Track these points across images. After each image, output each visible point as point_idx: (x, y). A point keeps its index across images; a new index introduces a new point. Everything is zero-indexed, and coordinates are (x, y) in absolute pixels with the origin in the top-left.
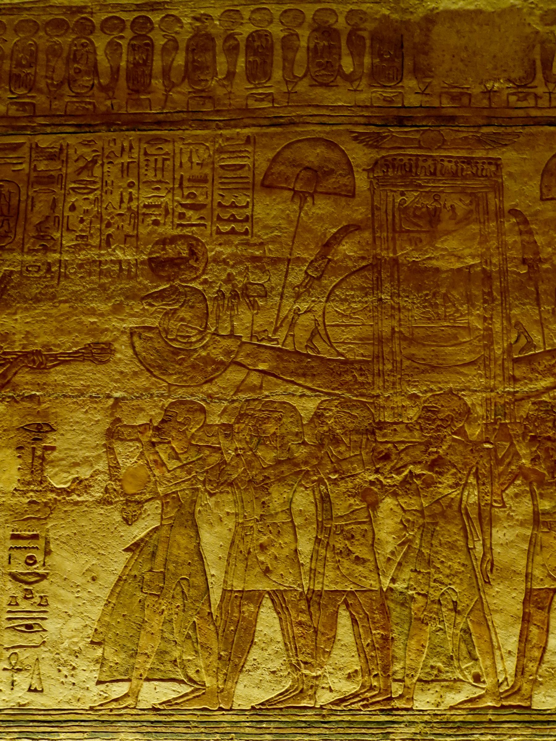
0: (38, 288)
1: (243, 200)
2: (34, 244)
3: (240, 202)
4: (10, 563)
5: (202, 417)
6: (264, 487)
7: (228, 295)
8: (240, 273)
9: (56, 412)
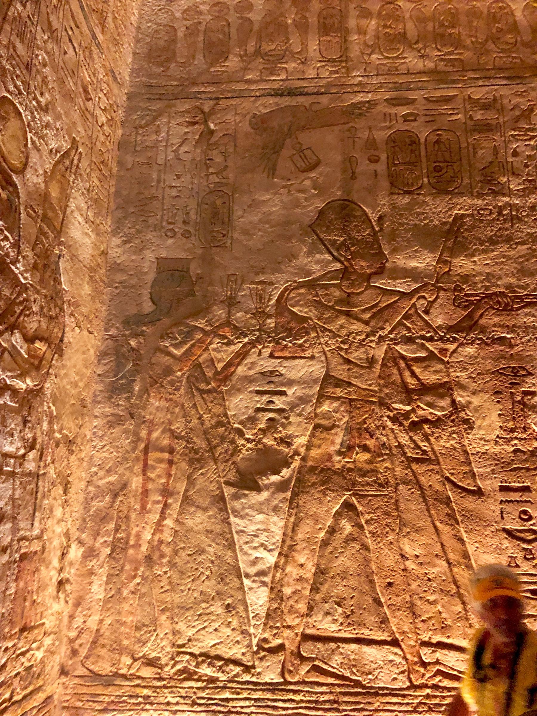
0: (492, 231)
2: (481, 188)
4: (503, 518)
9: (530, 355)
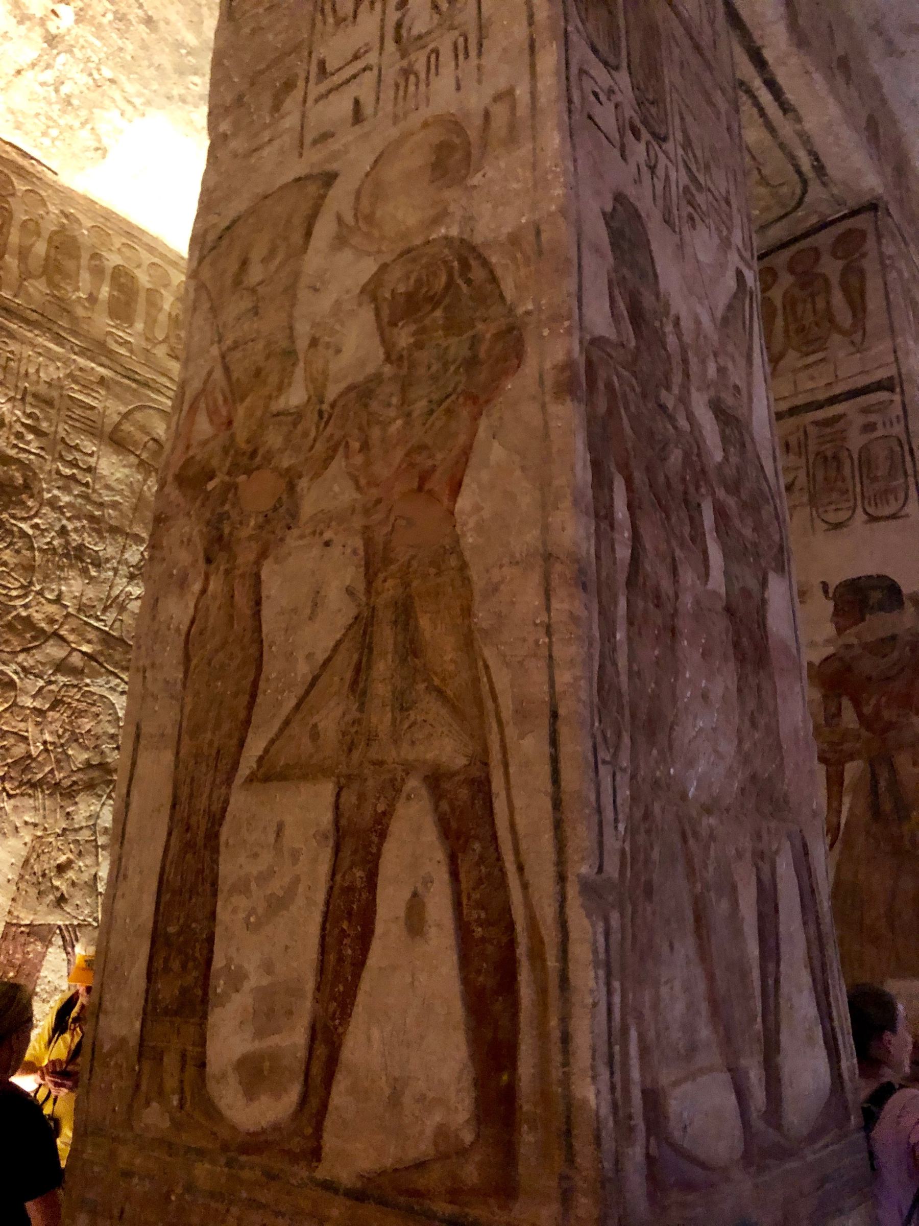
1: (90, 447)
3: (85, 447)
5: (13, 694)
6: (69, 793)
7: (60, 551)
8: (76, 530)
